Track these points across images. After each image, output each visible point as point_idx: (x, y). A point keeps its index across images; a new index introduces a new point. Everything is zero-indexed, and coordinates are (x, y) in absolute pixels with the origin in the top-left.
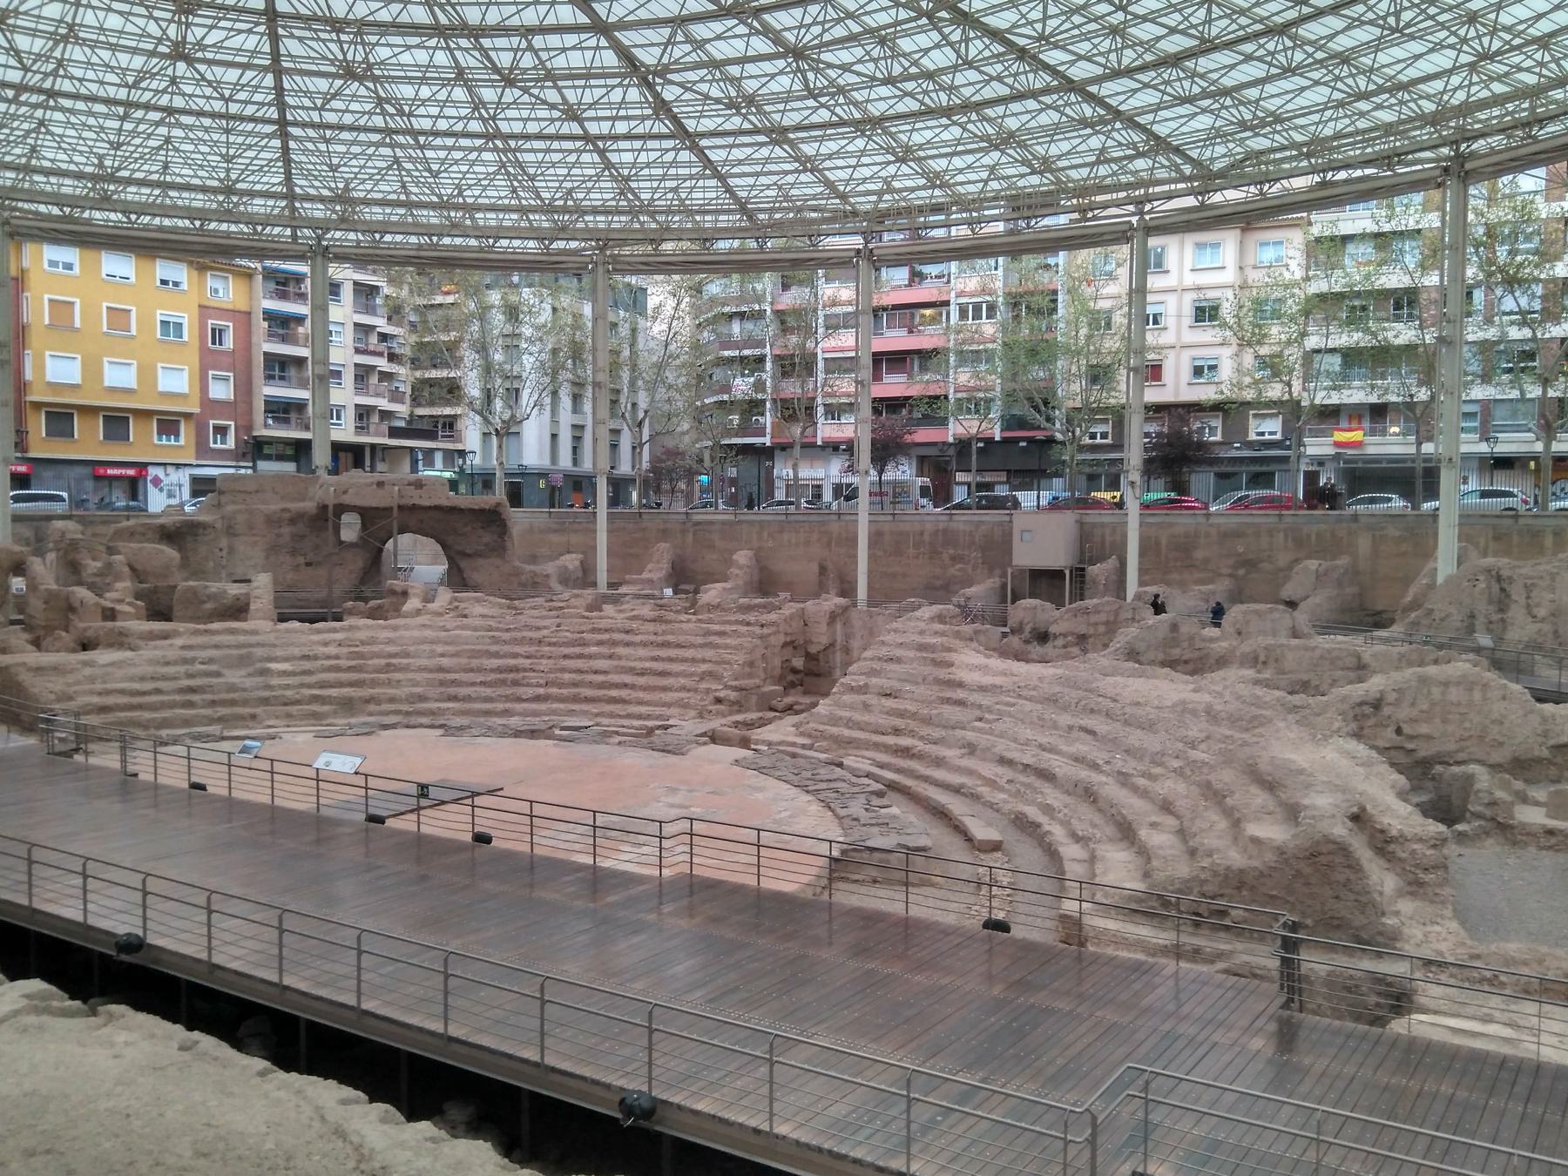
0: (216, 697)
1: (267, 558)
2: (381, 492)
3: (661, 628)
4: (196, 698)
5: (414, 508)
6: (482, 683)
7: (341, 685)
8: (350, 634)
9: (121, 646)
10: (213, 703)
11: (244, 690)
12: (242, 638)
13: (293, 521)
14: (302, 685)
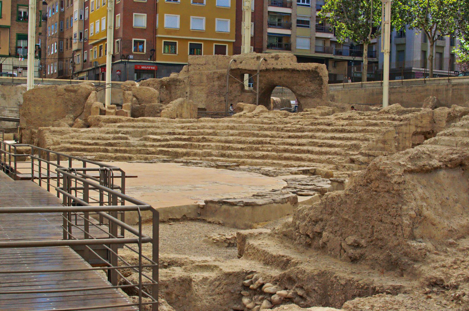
0: (118, 148)
1: (207, 97)
3: (345, 122)
4: (109, 148)
5: (274, 70)
6: (242, 149)
7: (178, 146)
8: (195, 124)
9: (96, 125)
10: (116, 151)
11: (133, 146)
12: (146, 124)
13: (219, 78)
14: (160, 146)
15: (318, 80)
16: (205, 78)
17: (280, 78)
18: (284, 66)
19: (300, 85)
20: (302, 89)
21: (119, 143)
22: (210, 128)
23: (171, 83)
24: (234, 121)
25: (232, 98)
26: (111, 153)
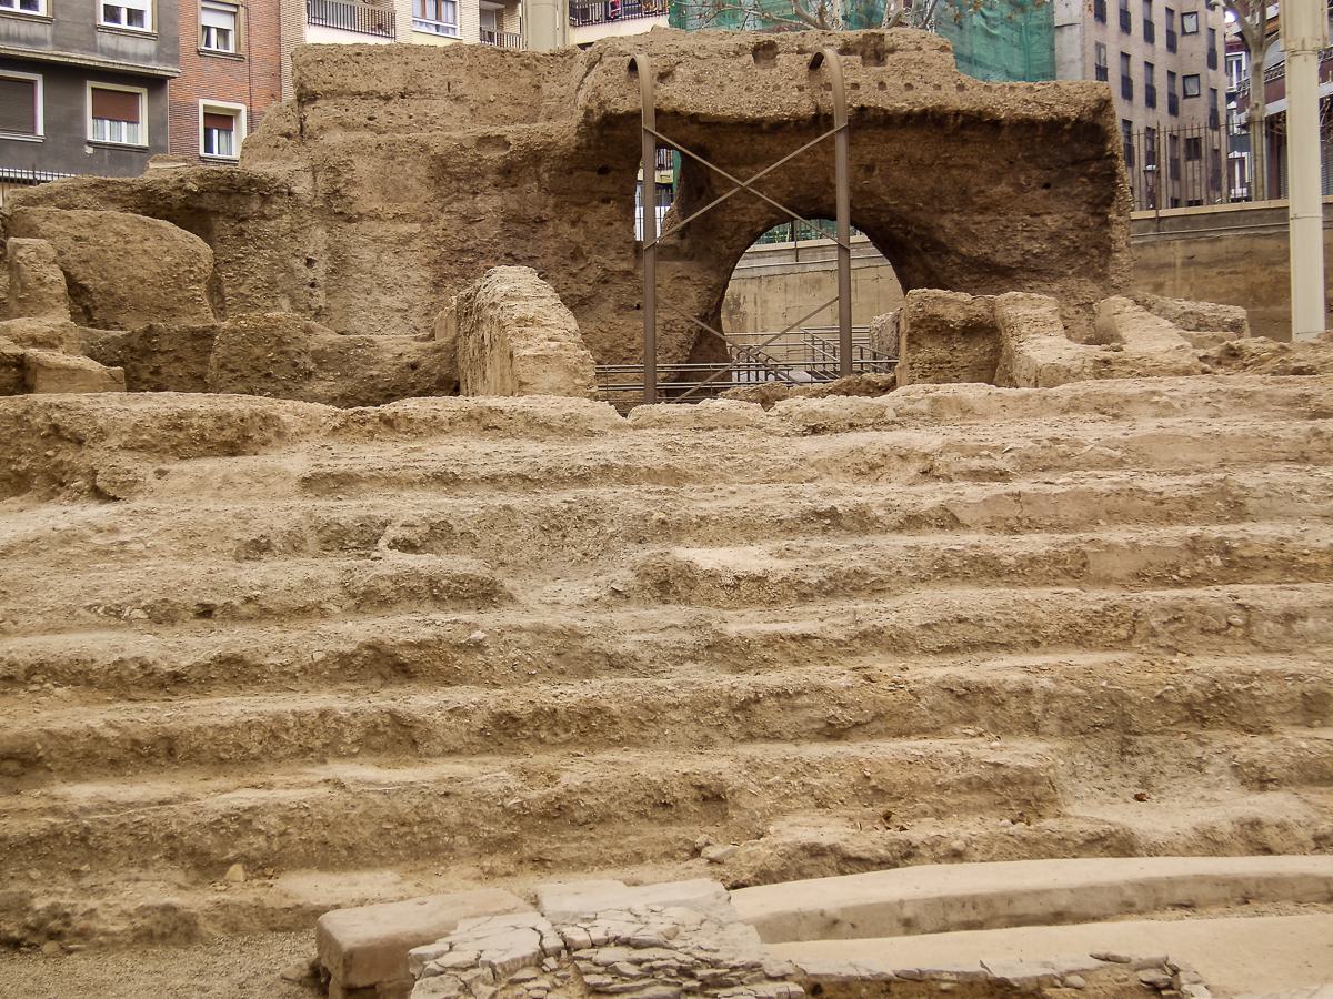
0: (517, 699)
1: (437, 286)
2: (764, 74)
4: (421, 702)
5: (867, 121)
9: (56, 483)
10: (505, 731)
11: (616, 663)
13: (508, 174)
15: (1092, 178)
16: (415, 174)
17: (870, 169)
18: (925, 98)
19: (984, 209)
20: (993, 228)
21: (479, 646)
23: (208, 202)
24: (1251, 395)
25: (586, 289)
26: (451, 752)
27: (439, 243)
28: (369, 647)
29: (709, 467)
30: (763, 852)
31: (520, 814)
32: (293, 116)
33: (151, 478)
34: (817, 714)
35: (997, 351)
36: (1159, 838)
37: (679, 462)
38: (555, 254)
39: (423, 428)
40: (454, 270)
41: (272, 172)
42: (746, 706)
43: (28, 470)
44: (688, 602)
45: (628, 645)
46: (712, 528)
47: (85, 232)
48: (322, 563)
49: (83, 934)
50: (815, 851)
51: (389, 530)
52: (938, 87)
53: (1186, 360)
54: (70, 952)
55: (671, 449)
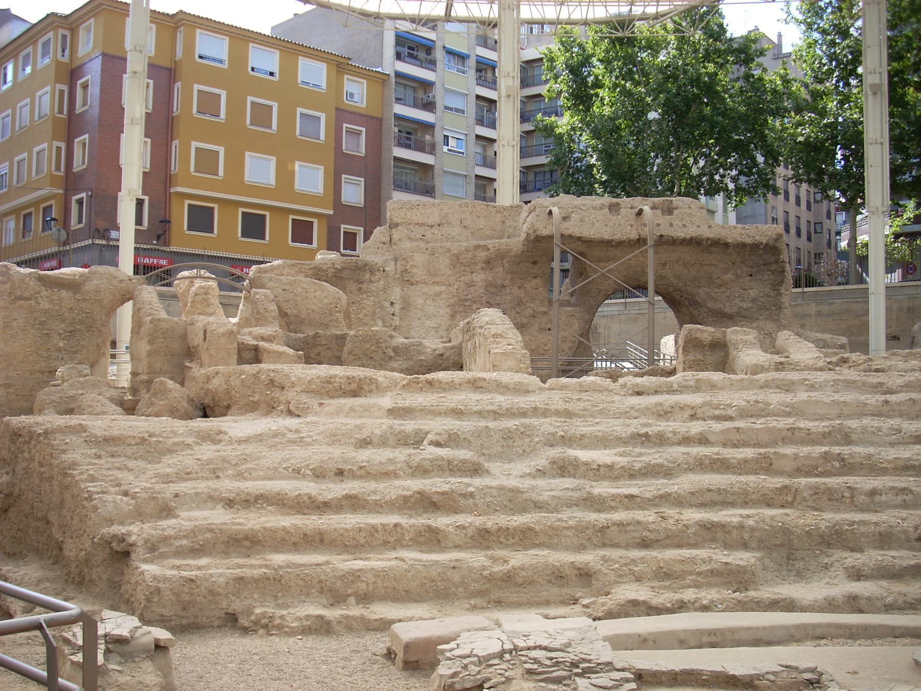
1: (453, 316)
4: (442, 521)
5: (663, 242)
9: (270, 408)
10: (483, 538)
11: (539, 506)
12: (502, 400)
15: (773, 272)
16: (443, 263)
17: (664, 265)
18: (691, 231)
19: (719, 286)
21: (471, 495)
22: (789, 415)
23: (346, 274)
24: (854, 382)
25: (525, 320)
26: (457, 547)
27: (454, 296)
28: (419, 493)
29: (585, 410)
30: (609, 602)
31: (491, 579)
32: (387, 234)
33: (316, 406)
34: (637, 535)
35: (727, 356)
36: (805, 603)
37: (570, 406)
38: (510, 303)
39: (446, 386)
40: (461, 309)
41: (376, 260)
42: (603, 529)
43: (258, 401)
44: (574, 477)
45: (545, 496)
46: (586, 440)
47: (288, 287)
48: (397, 451)
49: (280, 627)
50: (634, 603)
51: (429, 436)
52: (699, 226)
53: (821, 364)
54: (272, 635)
55: (567, 401)
